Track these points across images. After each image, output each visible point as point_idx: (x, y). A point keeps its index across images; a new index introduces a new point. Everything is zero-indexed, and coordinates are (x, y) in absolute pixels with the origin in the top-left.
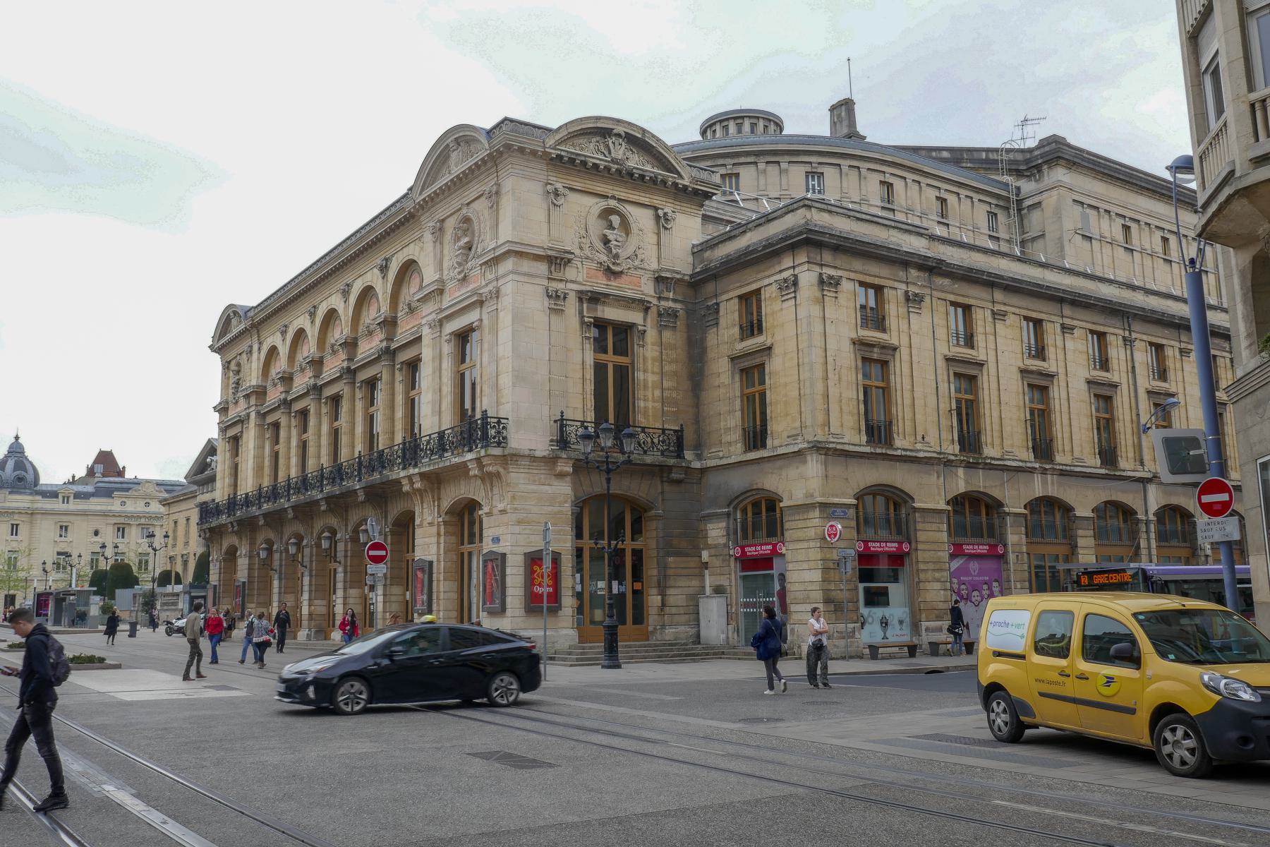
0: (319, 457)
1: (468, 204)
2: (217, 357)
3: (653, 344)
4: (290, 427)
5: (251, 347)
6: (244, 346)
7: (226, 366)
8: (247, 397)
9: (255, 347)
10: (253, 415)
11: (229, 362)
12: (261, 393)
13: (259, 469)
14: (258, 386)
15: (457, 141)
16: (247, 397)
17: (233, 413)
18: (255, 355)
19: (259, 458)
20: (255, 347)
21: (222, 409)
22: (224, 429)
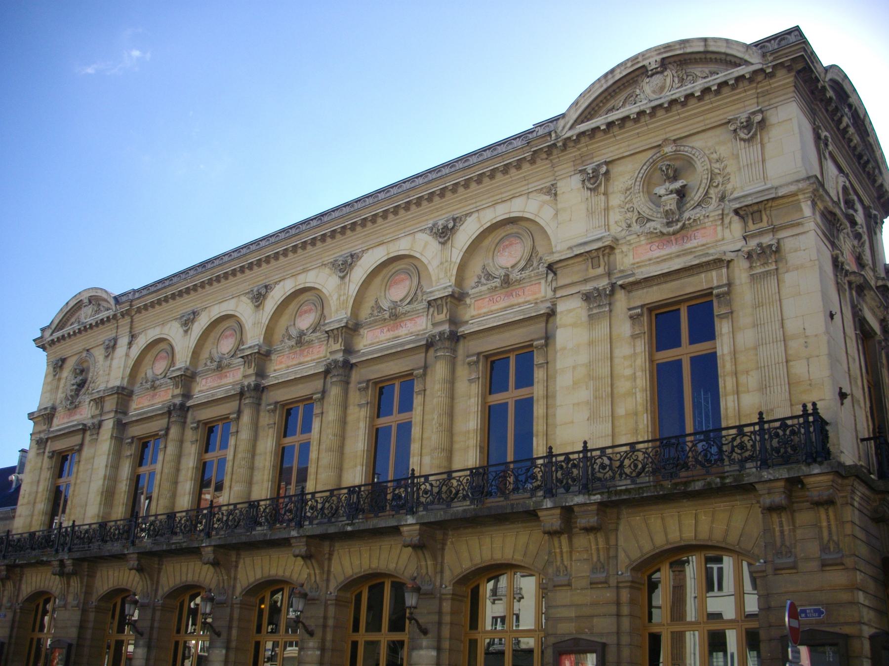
0: (250, 483)
1: (675, 141)
2: (42, 355)
3: (330, 450)
4: (181, 442)
5: (115, 340)
6: (104, 334)
7: (58, 365)
8: (99, 401)
9: (123, 341)
10: (108, 425)
11: (63, 360)
12: (124, 394)
13: (108, 494)
14: (123, 388)
15: (664, 64)
16: (99, 401)
17: (60, 422)
18: (121, 350)
19: (112, 480)
20: (123, 341)
21: (44, 416)
22: (40, 442)
